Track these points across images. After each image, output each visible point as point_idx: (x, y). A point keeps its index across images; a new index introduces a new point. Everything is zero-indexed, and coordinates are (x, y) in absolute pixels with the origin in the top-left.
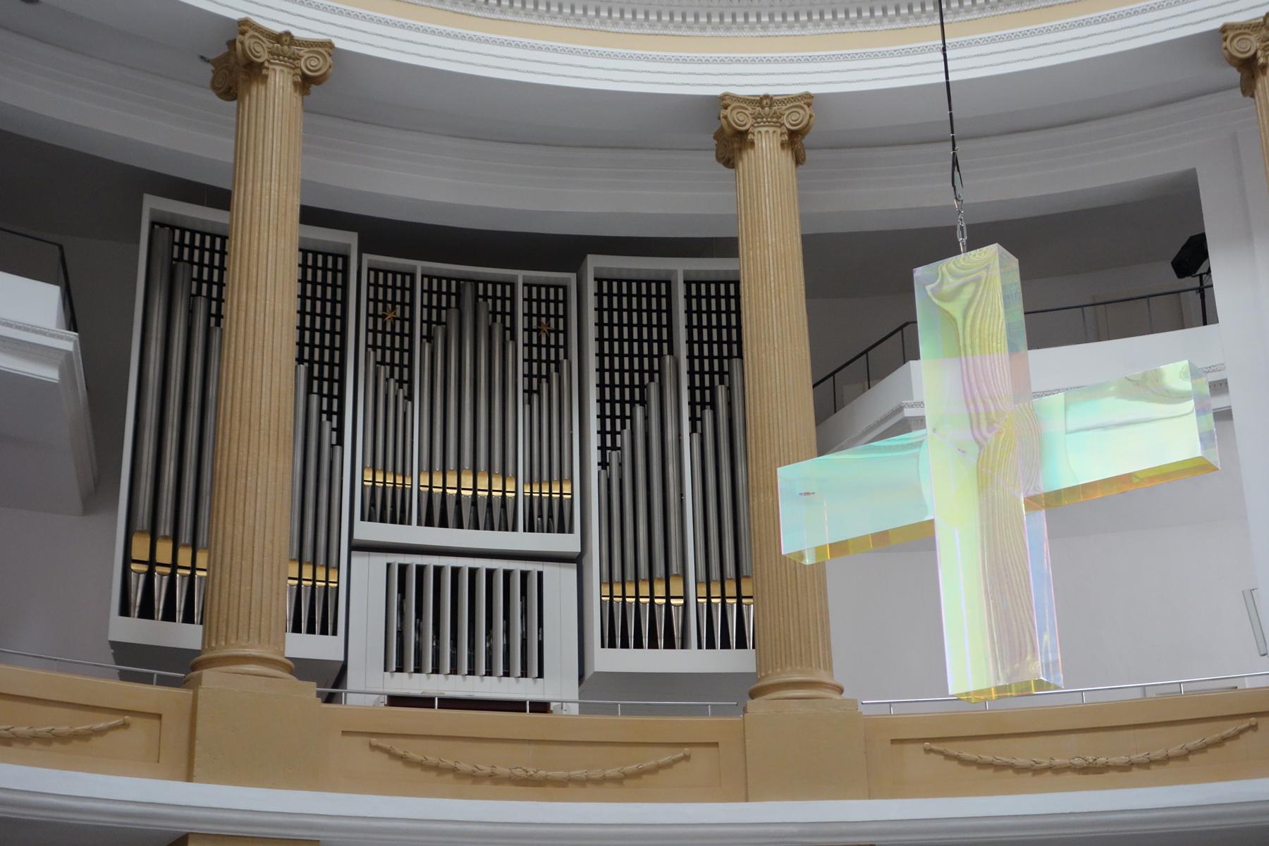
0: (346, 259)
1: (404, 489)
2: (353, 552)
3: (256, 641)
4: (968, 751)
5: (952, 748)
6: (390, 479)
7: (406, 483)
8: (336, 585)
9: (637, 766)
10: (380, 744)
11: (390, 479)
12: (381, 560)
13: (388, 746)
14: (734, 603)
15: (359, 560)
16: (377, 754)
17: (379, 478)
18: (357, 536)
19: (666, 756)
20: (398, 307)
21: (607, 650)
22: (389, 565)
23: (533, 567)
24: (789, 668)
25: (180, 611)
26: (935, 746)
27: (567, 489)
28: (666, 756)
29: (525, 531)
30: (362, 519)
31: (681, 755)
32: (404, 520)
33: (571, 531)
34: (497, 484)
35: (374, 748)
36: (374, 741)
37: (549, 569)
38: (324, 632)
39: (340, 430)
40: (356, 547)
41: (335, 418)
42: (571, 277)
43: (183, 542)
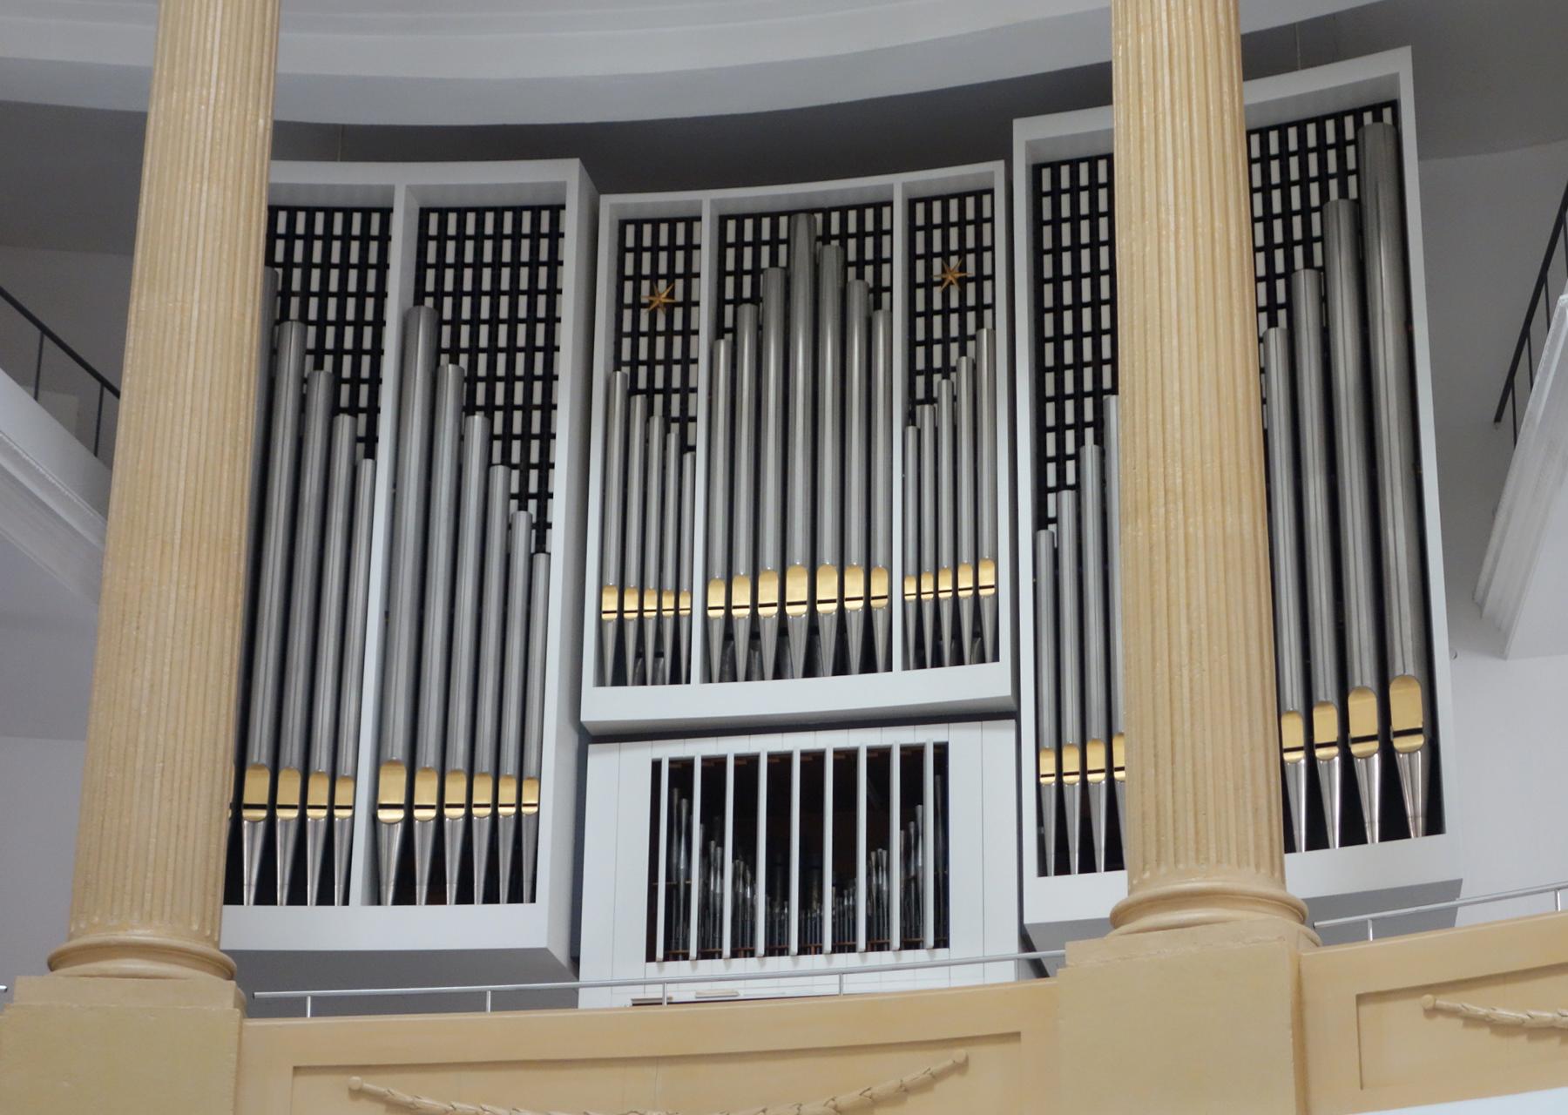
0: (557, 210)
1: (677, 618)
2: (592, 747)
3: (136, 915)
4: (1506, 1006)
5: (1474, 1002)
6: (650, 604)
7: (682, 606)
8: (535, 809)
9: (859, 1092)
10: (368, 1086)
11: (650, 604)
12: (639, 758)
13: (382, 1090)
14: (1299, 760)
15: (601, 760)
16: (364, 1103)
17: (631, 603)
18: (586, 716)
19: (914, 1067)
20: (662, 284)
21: (1053, 881)
22: (656, 766)
23: (926, 736)
24: (1163, 870)
25: (249, 885)
26: (1444, 1001)
27: (986, 577)
28: (914, 1067)
29: (906, 667)
30: (601, 681)
31: (949, 1063)
32: (677, 676)
33: (996, 658)
34: (855, 587)
35: (357, 1093)
36: (356, 1080)
37: (958, 737)
38: (515, 897)
39: (541, 526)
40: (590, 737)
41: (532, 504)
42: (998, 167)
43: (255, 759)
